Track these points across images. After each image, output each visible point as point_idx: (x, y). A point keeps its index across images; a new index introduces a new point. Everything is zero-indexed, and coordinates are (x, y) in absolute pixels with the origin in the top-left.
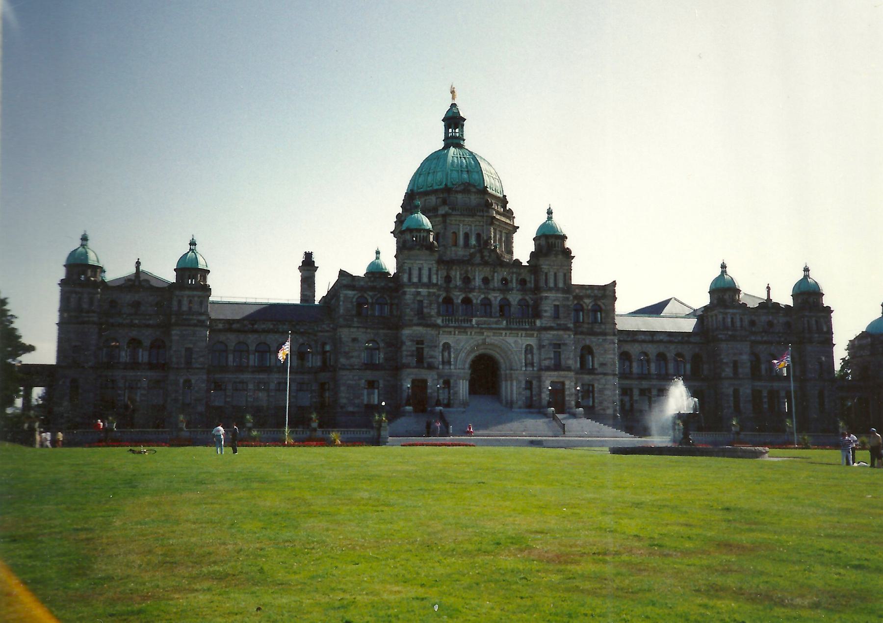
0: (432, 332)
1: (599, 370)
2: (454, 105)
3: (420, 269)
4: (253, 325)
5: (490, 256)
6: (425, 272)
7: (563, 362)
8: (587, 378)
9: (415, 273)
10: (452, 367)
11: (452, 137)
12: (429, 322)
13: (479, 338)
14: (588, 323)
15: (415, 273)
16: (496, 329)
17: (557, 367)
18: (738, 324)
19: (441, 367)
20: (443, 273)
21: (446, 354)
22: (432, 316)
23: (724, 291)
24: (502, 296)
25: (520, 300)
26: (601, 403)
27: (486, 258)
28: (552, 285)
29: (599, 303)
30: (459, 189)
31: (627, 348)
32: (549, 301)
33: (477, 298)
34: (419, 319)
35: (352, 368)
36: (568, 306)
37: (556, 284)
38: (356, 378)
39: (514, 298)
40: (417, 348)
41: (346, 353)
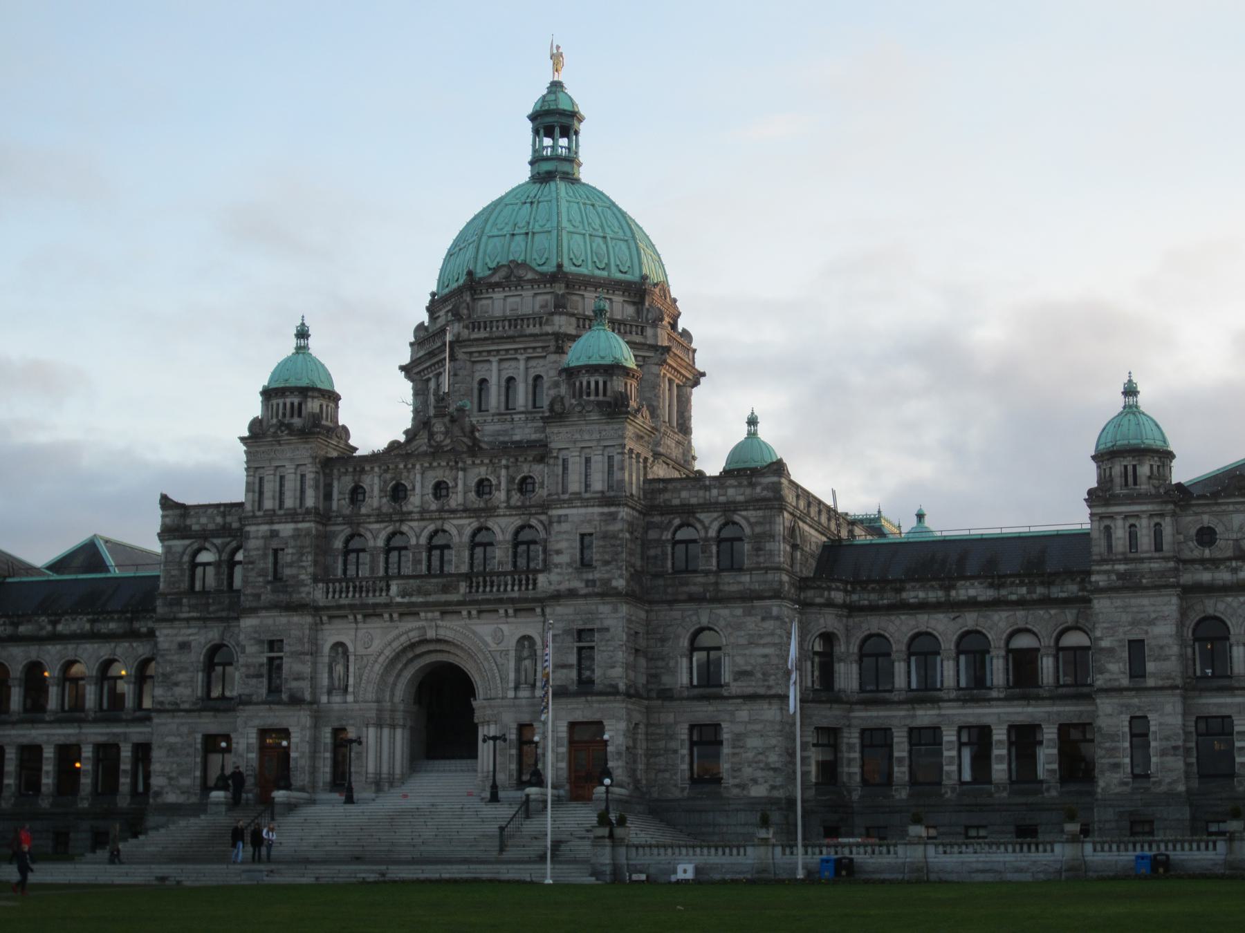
0: (301, 622)
1: (735, 688)
2: (556, 86)
3: (282, 478)
4: (54, 623)
5: (446, 433)
6: (291, 484)
7: (598, 673)
8: (705, 712)
9: (270, 487)
10: (350, 698)
11: (556, 158)
12: (295, 597)
13: (409, 629)
14: (707, 573)
15: (270, 487)
16: (436, 604)
17: (585, 687)
18: (1145, 541)
19: (324, 699)
20: (341, 485)
21: (339, 669)
22: (302, 584)
23: (1129, 462)
24: (475, 525)
25: (522, 528)
26: (736, 770)
27: (439, 438)
28: (575, 485)
29: (737, 518)
30: (495, 279)
31: (874, 624)
32: (565, 527)
33: (416, 533)
34: (273, 591)
35: (174, 709)
36: (615, 537)
37: (587, 486)
38: (185, 729)
39: (503, 527)
40: (271, 660)
41: (166, 676)
